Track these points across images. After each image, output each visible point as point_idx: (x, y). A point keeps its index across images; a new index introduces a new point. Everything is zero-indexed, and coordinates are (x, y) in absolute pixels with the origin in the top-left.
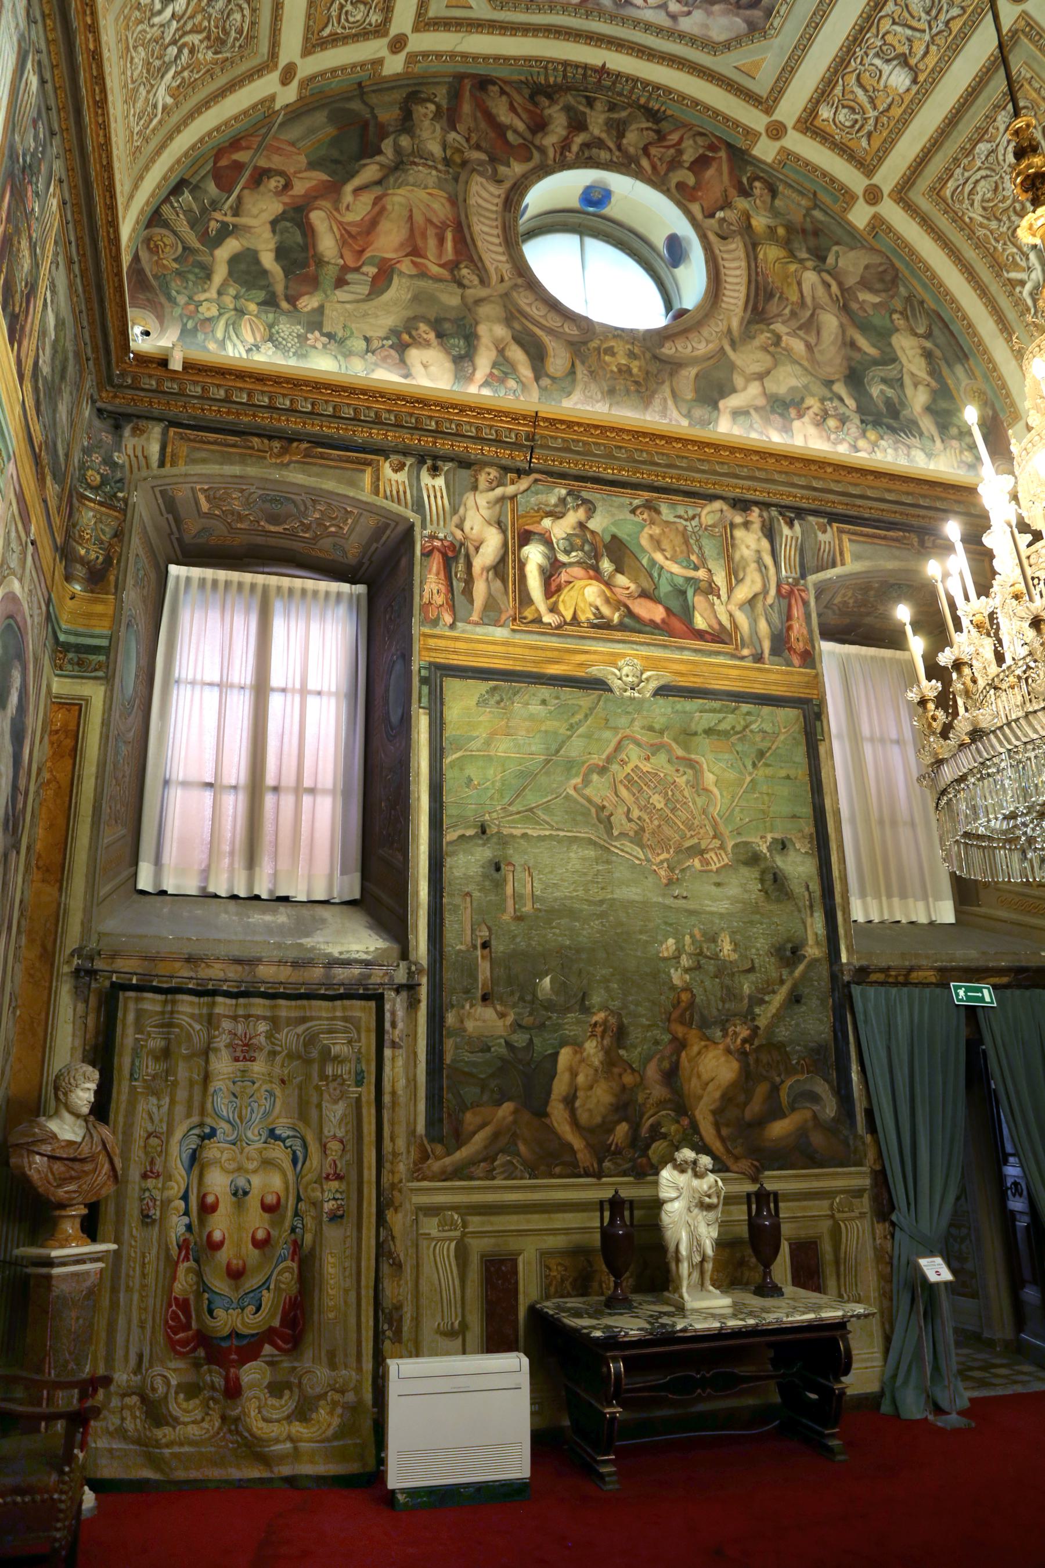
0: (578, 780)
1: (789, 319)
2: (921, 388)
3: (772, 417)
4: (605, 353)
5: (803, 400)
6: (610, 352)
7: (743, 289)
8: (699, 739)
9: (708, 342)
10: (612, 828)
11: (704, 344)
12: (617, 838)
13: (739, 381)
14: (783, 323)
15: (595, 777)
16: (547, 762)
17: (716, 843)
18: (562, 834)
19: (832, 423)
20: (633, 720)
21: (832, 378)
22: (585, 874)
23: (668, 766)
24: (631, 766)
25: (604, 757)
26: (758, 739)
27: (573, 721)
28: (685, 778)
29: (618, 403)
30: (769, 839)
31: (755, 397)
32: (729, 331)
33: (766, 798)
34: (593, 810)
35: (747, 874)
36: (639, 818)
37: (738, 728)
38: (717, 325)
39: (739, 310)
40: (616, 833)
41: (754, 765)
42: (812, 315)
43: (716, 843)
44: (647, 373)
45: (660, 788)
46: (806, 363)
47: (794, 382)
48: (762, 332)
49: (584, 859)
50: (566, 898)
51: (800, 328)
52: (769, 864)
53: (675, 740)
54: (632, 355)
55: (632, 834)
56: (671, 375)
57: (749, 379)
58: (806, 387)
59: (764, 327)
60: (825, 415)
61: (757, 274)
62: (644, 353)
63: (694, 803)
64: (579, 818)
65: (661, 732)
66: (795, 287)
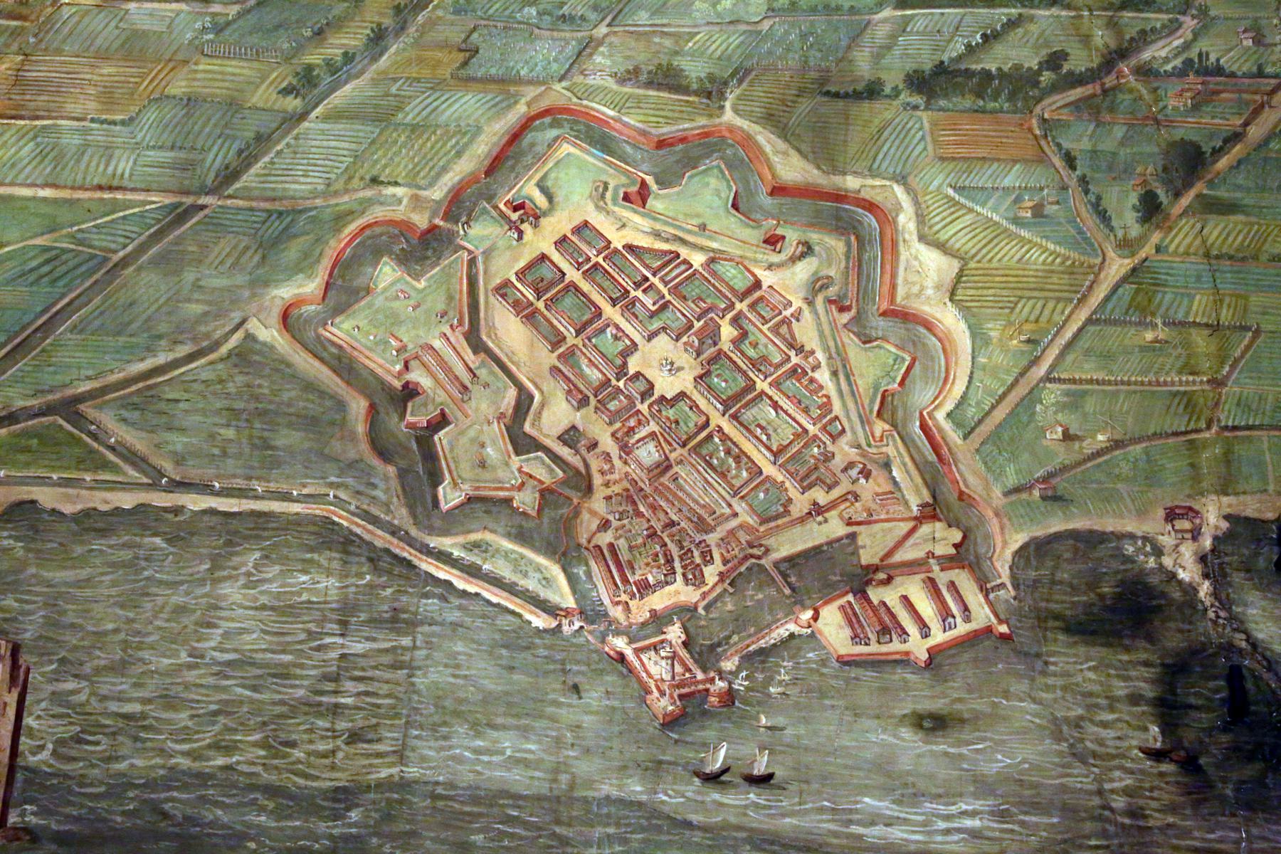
0: (310, 286)
8: (882, 111)
10: (435, 478)
12: (452, 521)
15: (387, 273)
16: (180, 215)
17: (943, 538)
18: (195, 503)
20: (587, 47)
22: (283, 674)
23: (733, 223)
24: (559, 224)
25: (438, 193)
26: (1174, 100)
27: (314, 57)
28: (803, 271)
30: (1213, 515)
33: (1200, 340)
34: (358, 406)
35: (1088, 677)
36: (570, 436)
37: (1079, 61)
40: (449, 496)
41: (1150, 209)
43: (943, 538)
45: (681, 311)
49: (286, 609)
50: (174, 779)
52: (1208, 629)
53: (771, 119)
55: (526, 500)
63: (842, 369)
64: (287, 438)
65: (712, 92)
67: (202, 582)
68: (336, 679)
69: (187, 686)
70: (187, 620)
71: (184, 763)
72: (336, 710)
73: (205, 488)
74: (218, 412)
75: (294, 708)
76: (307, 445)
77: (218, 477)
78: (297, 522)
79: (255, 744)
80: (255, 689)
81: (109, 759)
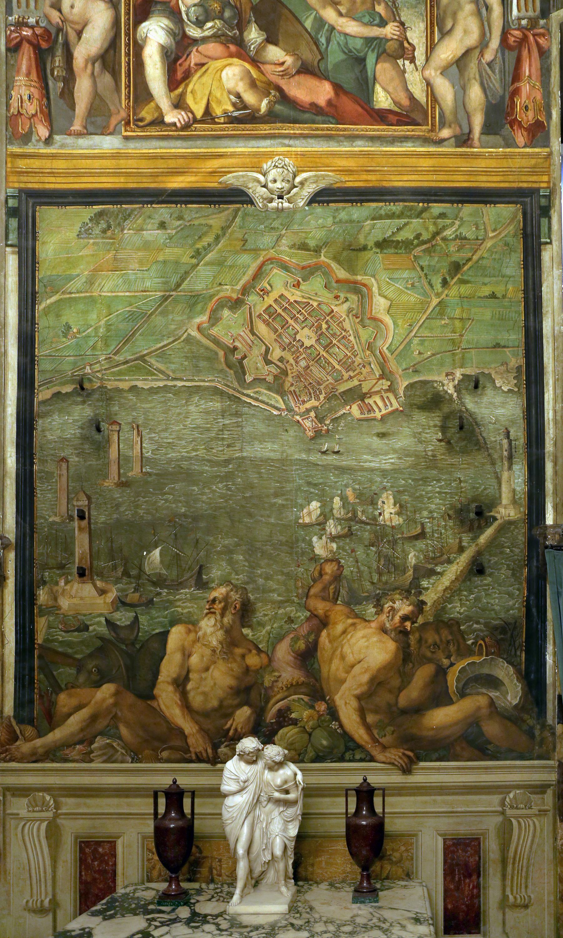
0: (204, 318)
8: (367, 255)
10: (244, 374)
12: (250, 385)
15: (226, 313)
16: (165, 298)
17: (385, 384)
18: (179, 384)
20: (280, 238)
22: (208, 430)
23: (325, 293)
24: (275, 295)
25: (238, 287)
26: (452, 248)
27: (199, 246)
28: (346, 306)
30: (458, 375)
33: (458, 323)
34: (221, 353)
36: (281, 359)
37: (425, 236)
40: (249, 379)
41: (445, 283)
50: (183, 458)
52: (456, 406)
53: (335, 259)
55: (270, 379)
63: (357, 336)
64: (202, 364)
65: (317, 250)
67: (184, 406)
68: (222, 431)
69: (183, 434)
70: (181, 416)
71: (186, 454)
72: (223, 439)
73: (182, 380)
74: (183, 357)
75: (212, 439)
76: (208, 366)
77: (185, 376)
78: (207, 388)
79: (203, 449)
80: (201, 434)
81: (166, 454)
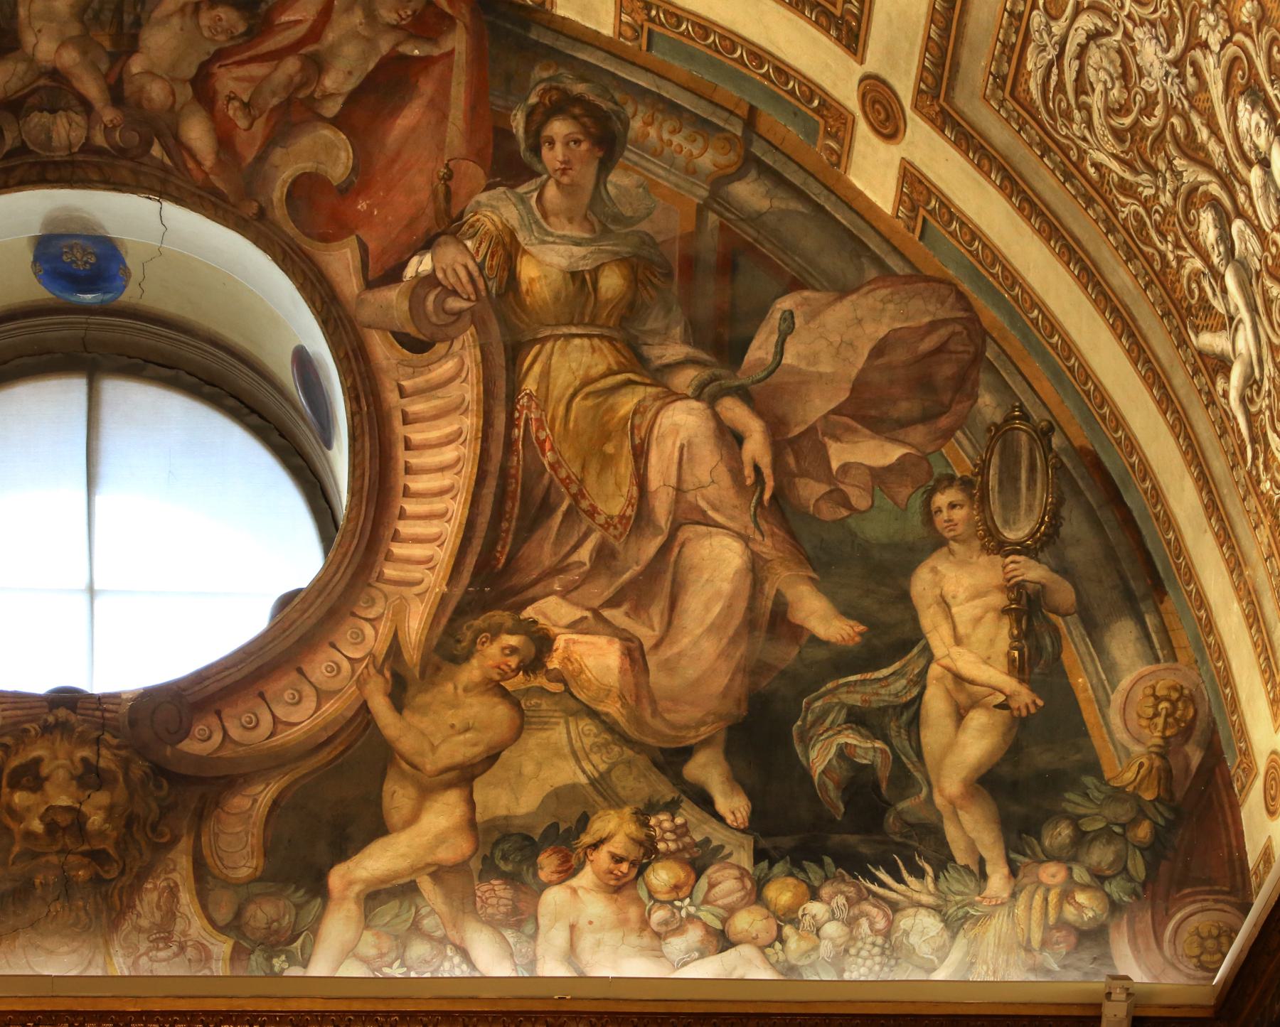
1: (588, 577)
2: (977, 719)
3: (482, 889)
4: (15, 785)
5: (583, 822)
6: (31, 777)
7: (457, 508)
9: (322, 696)
11: (310, 703)
13: (398, 797)
14: (565, 594)
19: (662, 876)
21: (691, 738)
29: (33, 925)
31: (440, 839)
32: (395, 649)
38: (359, 638)
39: (435, 581)
42: (664, 549)
44: (130, 821)
46: (613, 709)
47: (567, 773)
48: (495, 632)
51: (613, 603)
54: (90, 777)
56: (200, 817)
57: (427, 790)
58: (600, 784)
59: (500, 616)
60: (647, 853)
61: (509, 444)
62: (126, 764)
66: (625, 467)
